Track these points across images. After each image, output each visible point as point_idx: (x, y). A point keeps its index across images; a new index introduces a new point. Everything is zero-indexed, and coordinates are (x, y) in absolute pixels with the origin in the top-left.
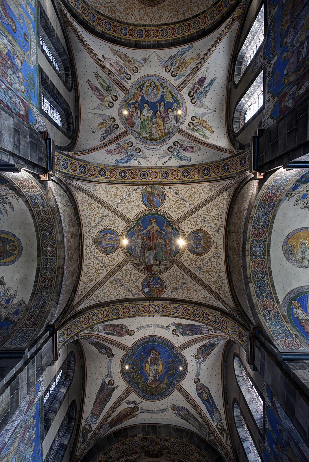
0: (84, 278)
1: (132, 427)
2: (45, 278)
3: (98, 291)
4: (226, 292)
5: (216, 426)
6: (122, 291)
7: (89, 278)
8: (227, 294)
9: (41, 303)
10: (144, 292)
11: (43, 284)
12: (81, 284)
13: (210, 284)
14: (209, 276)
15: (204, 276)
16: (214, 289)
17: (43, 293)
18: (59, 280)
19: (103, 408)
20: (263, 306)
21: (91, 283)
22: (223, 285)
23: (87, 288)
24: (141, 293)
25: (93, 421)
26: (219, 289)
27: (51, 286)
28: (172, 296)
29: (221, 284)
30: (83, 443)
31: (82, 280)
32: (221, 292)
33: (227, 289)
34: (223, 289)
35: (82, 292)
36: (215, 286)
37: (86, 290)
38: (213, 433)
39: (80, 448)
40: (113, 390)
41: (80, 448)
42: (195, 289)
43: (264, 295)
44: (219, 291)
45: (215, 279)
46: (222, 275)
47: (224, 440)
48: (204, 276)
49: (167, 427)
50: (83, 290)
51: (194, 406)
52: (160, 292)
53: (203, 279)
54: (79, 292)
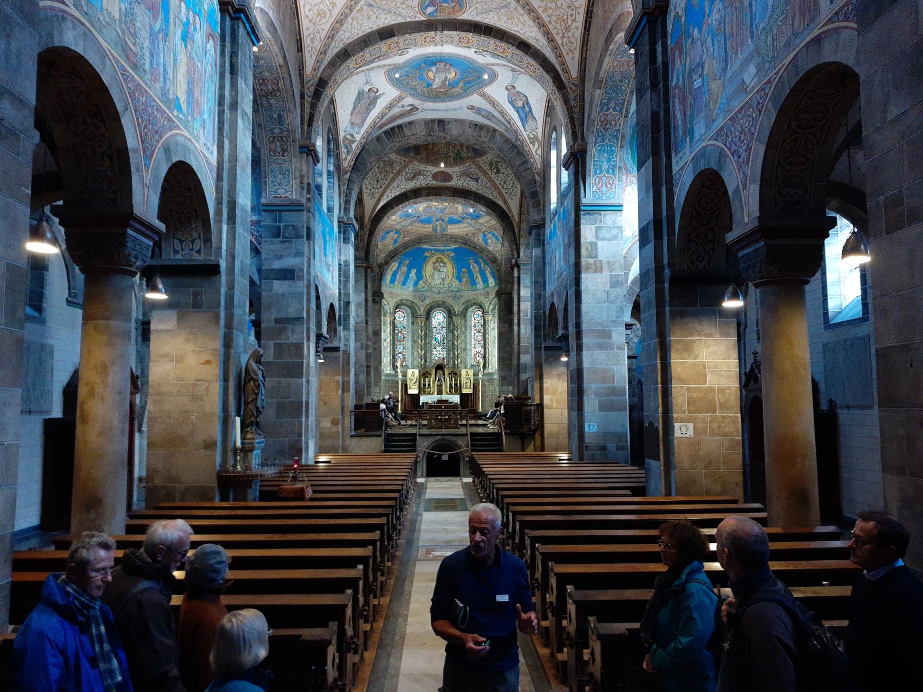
0: (307, 9)
1: (410, 123)
2: (263, 80)
3: (341, 32)
4: (572, 40)
5: (528, 136)
6: (383, 16)
7: (317, 7)
8: (574, 46)
9: (275, 116)
10: (425, 14)
11: (263, 87)
12: (305, 23)
13: (550, 22)
14: (553, 5)
15: (543, 4)
16: (554, 32)
17: (273, 101)
18: (288, 82)
19: (366, 117)
20: (602, 122)
21: (324, 20)
22: (575, 24)
23: (318, 32)
24: (419, 15)
25: (356, 130)
26: (563, 34)
27: (278, 89)
28: (478, 19)
29: (570, 22)
30: (348, 153)
31: (303, 16)
32: (565, 40)
33: (578, 34)
34: (570, 34)
35: (312, 41)
36: (558, 26)
37: (318, 36)
38: (522, 141)
39: (346, 159)
40: (377, 98)
41: (346, 159)
42: (522, 20)
43: (612, 105)
44: (563, 37)
45: (563, 11)
46: (577, 5)
47: (534, 150)
48: (543, 4)
49: (461, 122)
50: (312, 36)
51: (502, 113)
52: (454, 12)
53: (540, 11)
54: (307, 42)
